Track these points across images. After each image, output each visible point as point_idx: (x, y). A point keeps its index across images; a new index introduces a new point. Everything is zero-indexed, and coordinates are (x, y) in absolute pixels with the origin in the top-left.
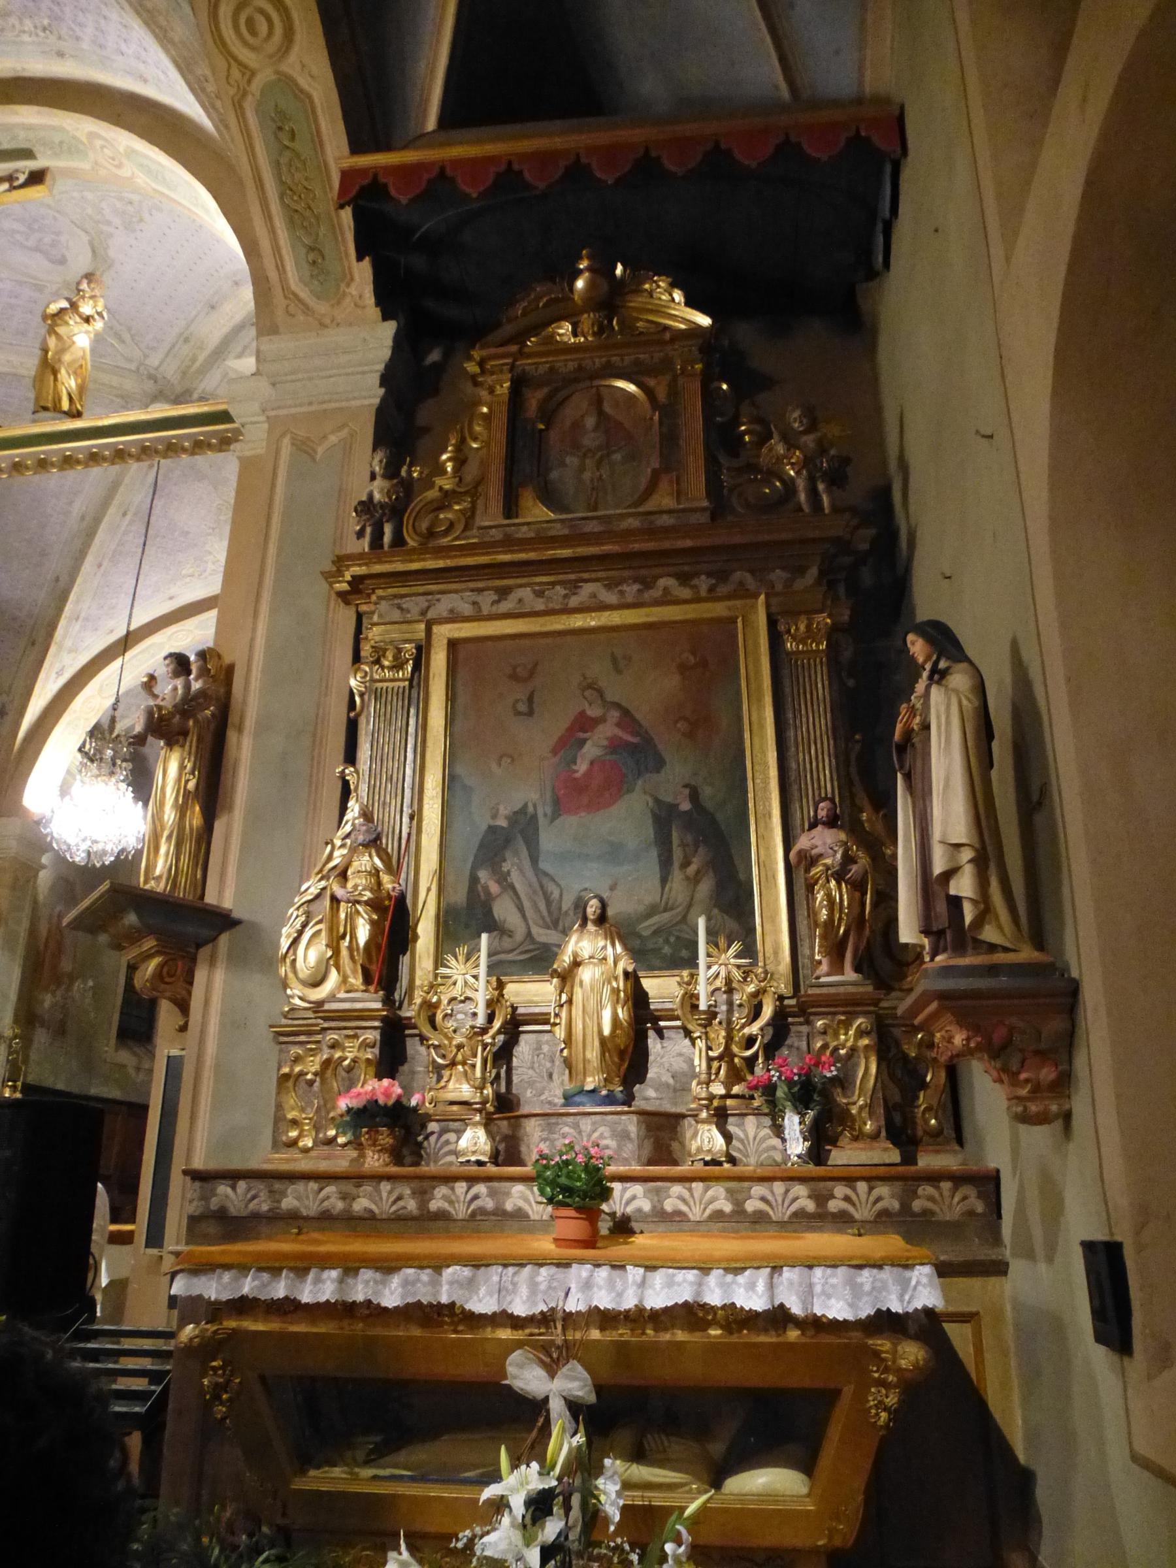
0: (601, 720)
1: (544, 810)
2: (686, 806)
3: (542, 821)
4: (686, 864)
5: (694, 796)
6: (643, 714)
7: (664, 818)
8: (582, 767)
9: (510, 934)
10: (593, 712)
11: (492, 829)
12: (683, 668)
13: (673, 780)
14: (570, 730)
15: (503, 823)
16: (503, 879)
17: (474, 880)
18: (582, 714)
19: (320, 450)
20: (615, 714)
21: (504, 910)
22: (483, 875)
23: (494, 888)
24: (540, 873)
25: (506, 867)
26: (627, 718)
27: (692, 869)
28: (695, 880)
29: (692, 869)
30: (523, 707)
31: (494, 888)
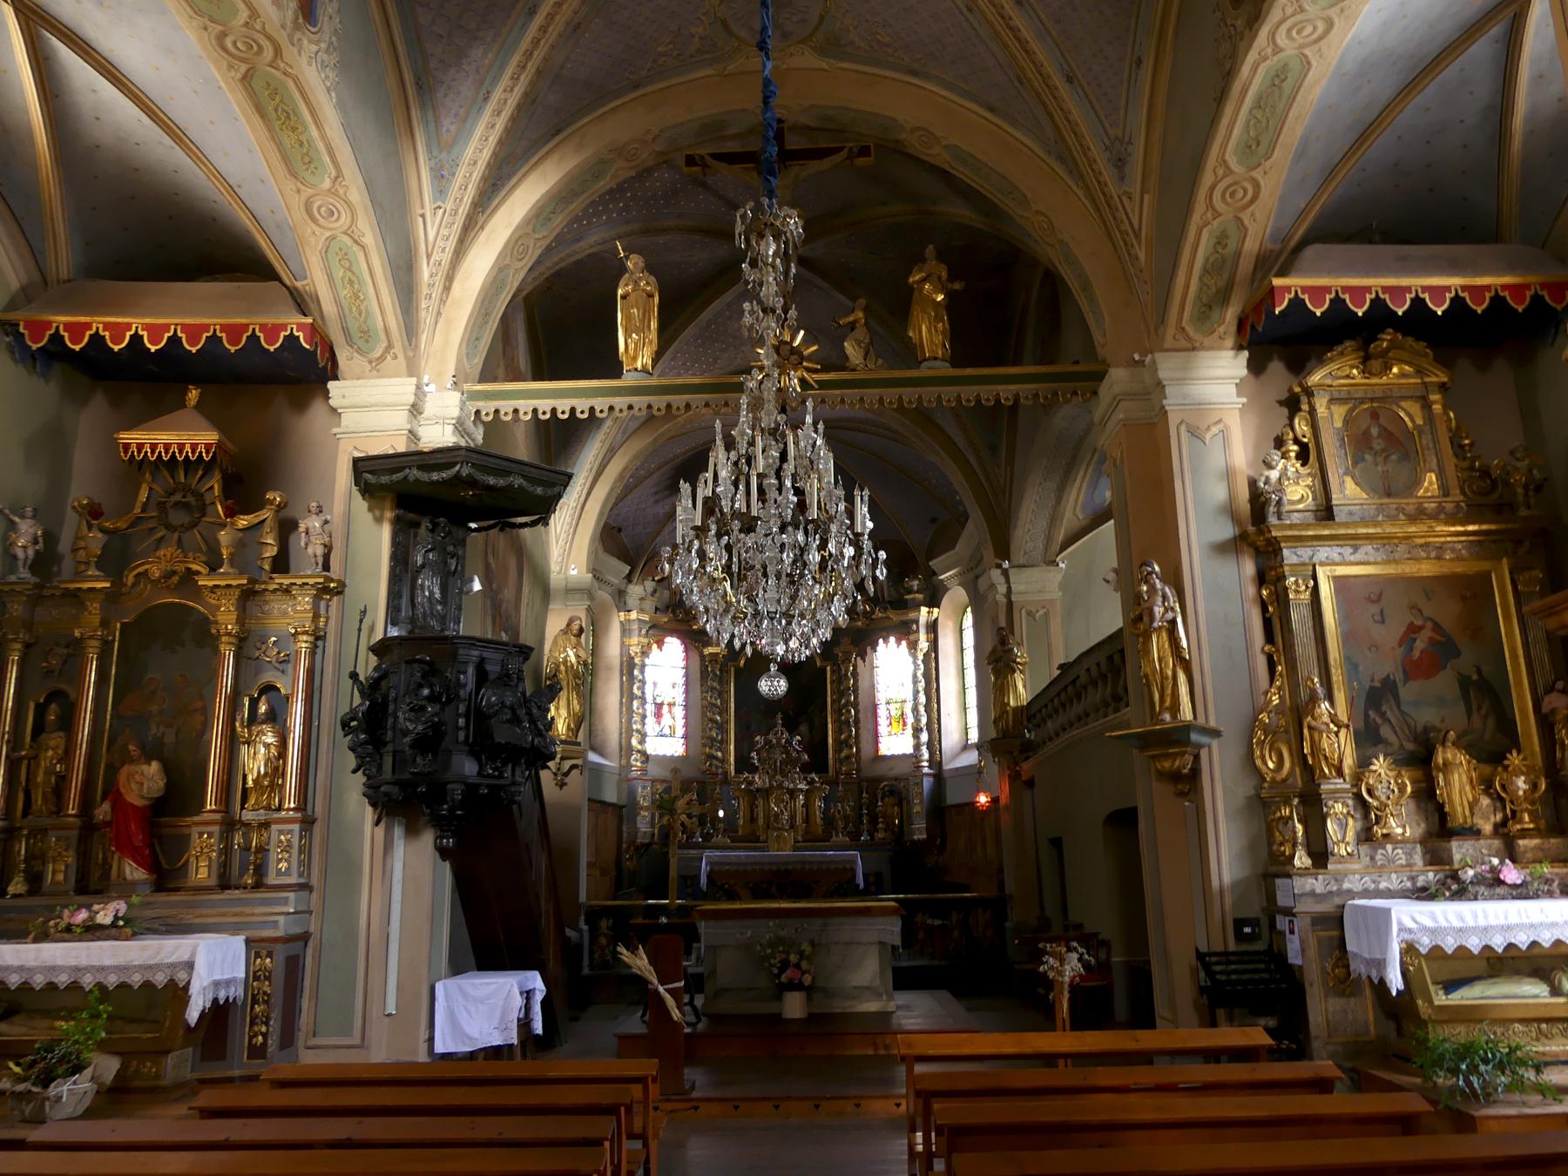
0: (1421, 628)
1: (1399, 677)
2: (1475, 677)
3: (1400, 685)
4: (1479, 709)
5: (1479, 671)
6: (1446, 625)
7: (1464, 684)
8: (1416, 654)
9: (1391, 745)
10: (1419, 622)
11: (1372, 688)
12: (1463, 598)
13: (1467, 661)
14: (1406, 633)
15: (1377, 684)
16: (1383, 715)
17: (1367, 715)
18: (1412, 623)
19: (1208, 436)
20: (1429, 624)
21: (1386, 732)
22: (1372, 714)
23: (1379, 721)
24: (1403, 713)
25: (1384, 708)
26: (1437, 627)
27: (1483, 712)
28: (1486, 717)
29: (1483, 712)
30: (1377, 618)
31: (1379, 721)
